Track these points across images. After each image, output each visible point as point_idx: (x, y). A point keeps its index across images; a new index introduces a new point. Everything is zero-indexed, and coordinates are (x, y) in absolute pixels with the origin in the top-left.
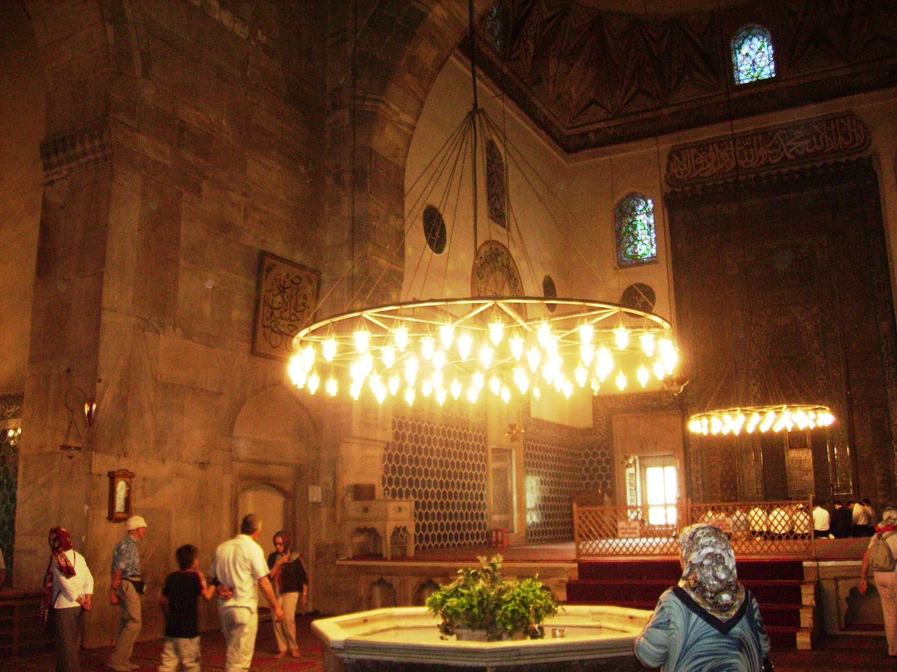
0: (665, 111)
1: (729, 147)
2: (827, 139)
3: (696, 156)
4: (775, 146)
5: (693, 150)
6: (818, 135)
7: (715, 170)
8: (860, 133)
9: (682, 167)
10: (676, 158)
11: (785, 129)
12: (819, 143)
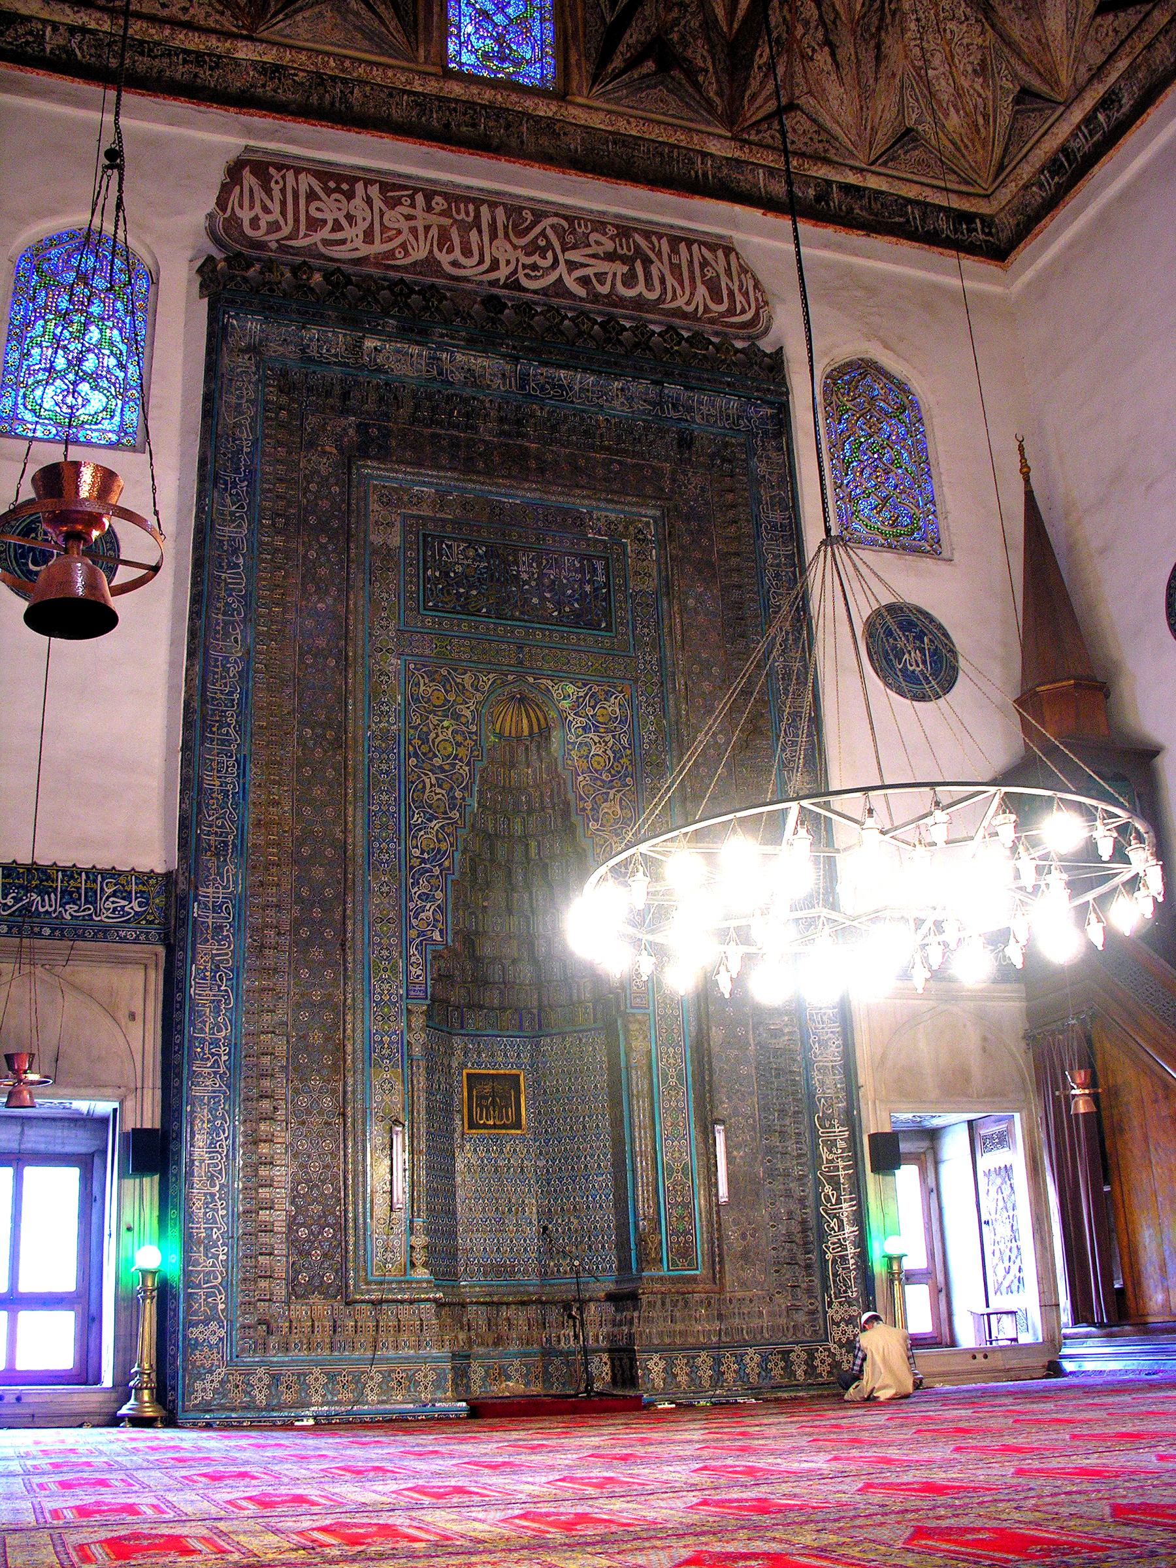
0: (244, 52)
1: (413, 206)
2: (670, 281)
3: (312, 196)
4: (532, 249)
5: (306, 182)
6: (647, 262)
7: (365, 250)
8: (746, 295)
9: (266, 210)
10: (249, 179)
11: (565, 218)
12: (649, 285)
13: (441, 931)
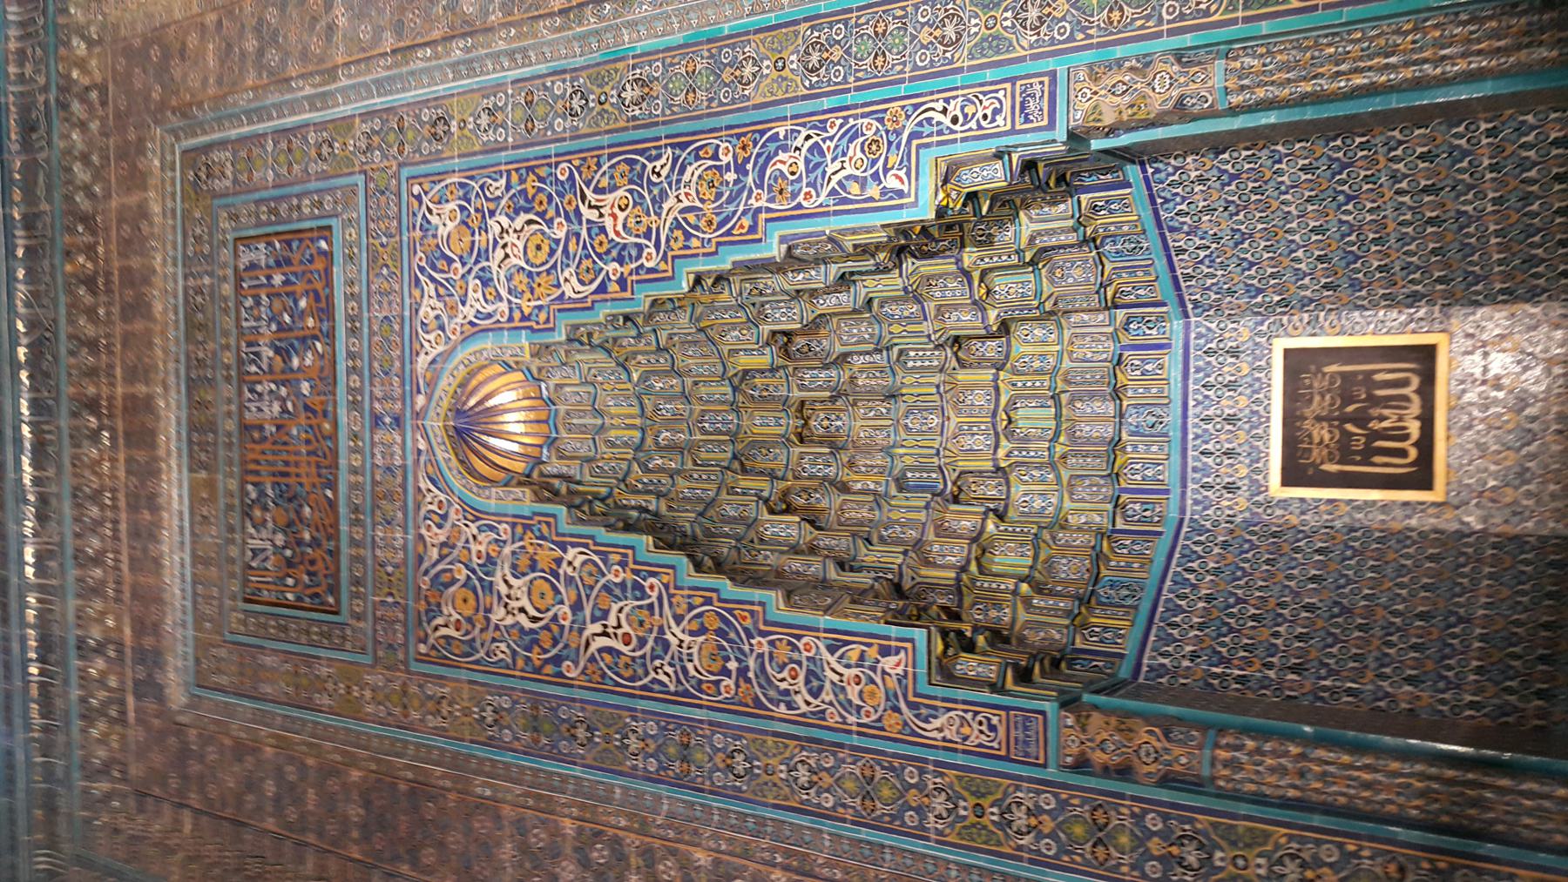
13: (885, 652)
